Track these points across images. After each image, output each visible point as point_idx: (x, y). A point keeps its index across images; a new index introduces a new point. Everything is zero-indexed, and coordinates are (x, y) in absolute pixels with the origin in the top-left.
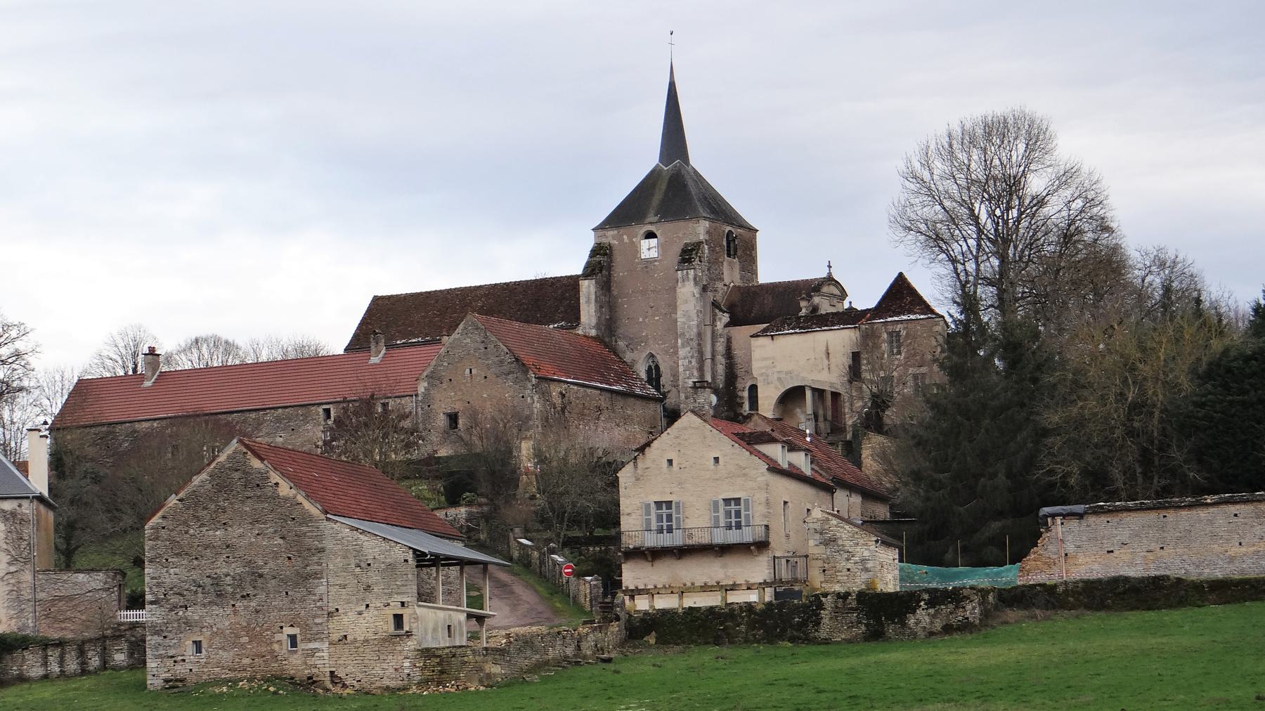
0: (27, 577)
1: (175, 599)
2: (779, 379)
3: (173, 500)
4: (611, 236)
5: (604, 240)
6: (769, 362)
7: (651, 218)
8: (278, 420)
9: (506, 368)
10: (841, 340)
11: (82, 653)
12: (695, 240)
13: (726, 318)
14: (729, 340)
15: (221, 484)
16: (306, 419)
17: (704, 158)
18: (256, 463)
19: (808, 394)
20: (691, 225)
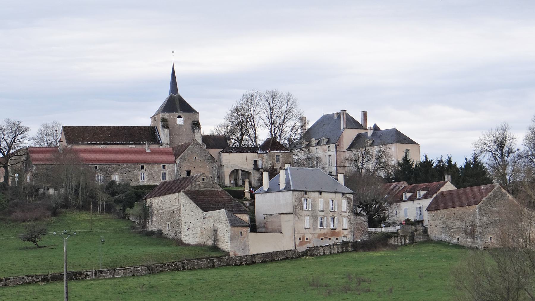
0: (352, 217)
1: (485, 226)
3: (484, 199)
6: (228, 161)
8: (124, 168)
9: (207, 158)
10: (251, 156)
11: (401, 239)
15: (496, 195)
16: (135, 168)
18: (504, 190)
19: (240, 172)
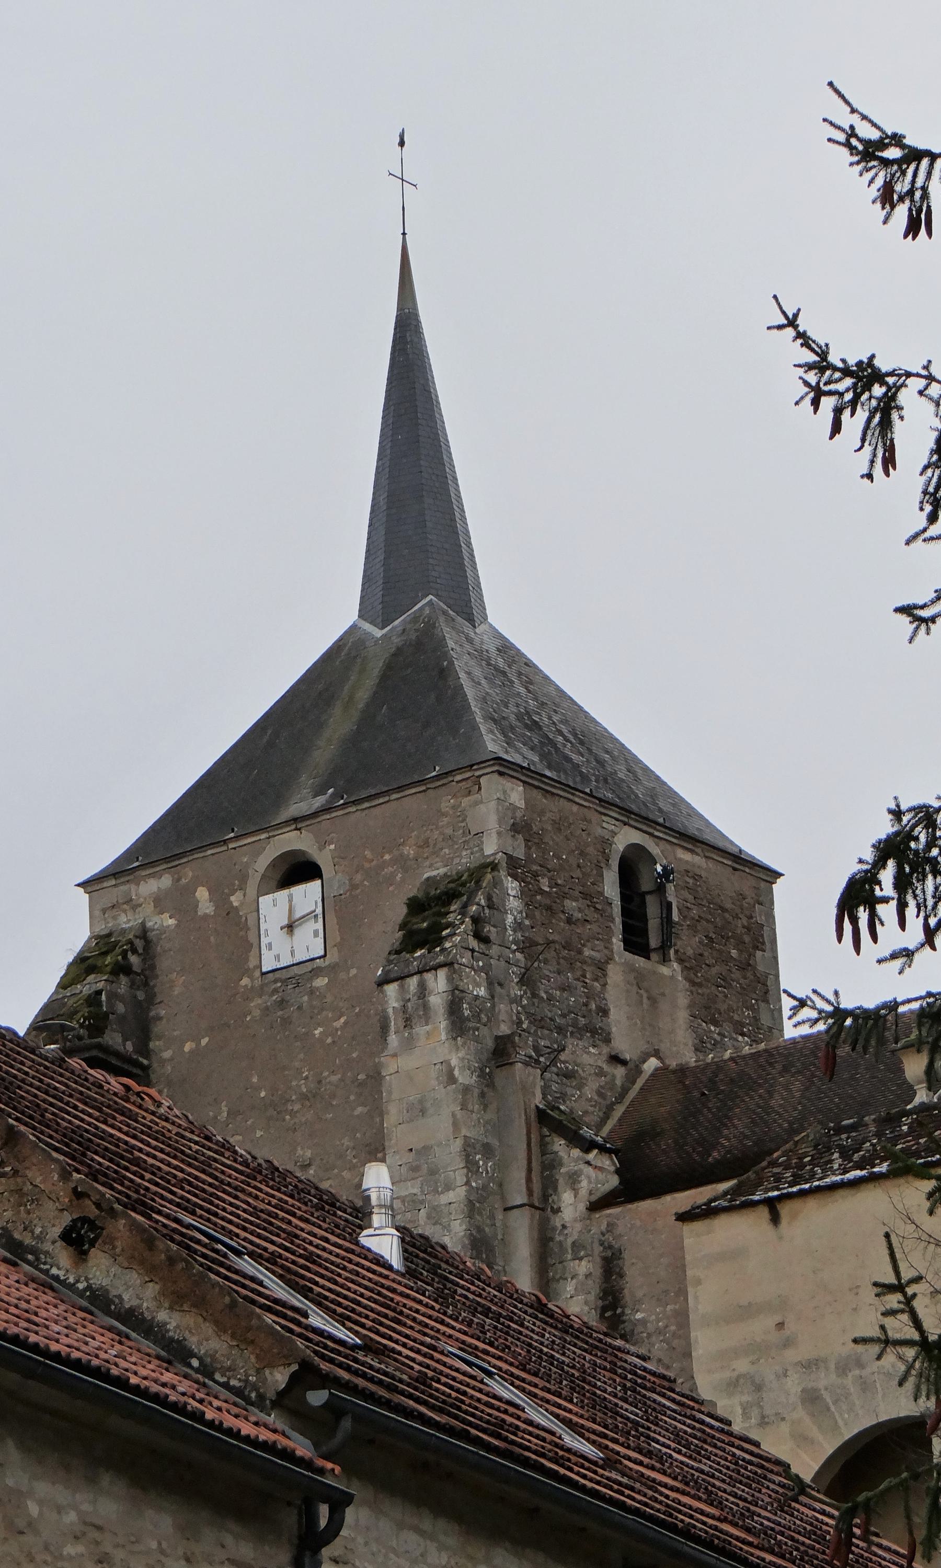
2: (811, 1398)
4: (148, 905)
5: (126, 921)
6: (760, 1328)
7: (302, 803)
12: (465, 860)
13: (599, 1173)
14: (611, 1266)
17: (540, 600)
20: (447, 803)
